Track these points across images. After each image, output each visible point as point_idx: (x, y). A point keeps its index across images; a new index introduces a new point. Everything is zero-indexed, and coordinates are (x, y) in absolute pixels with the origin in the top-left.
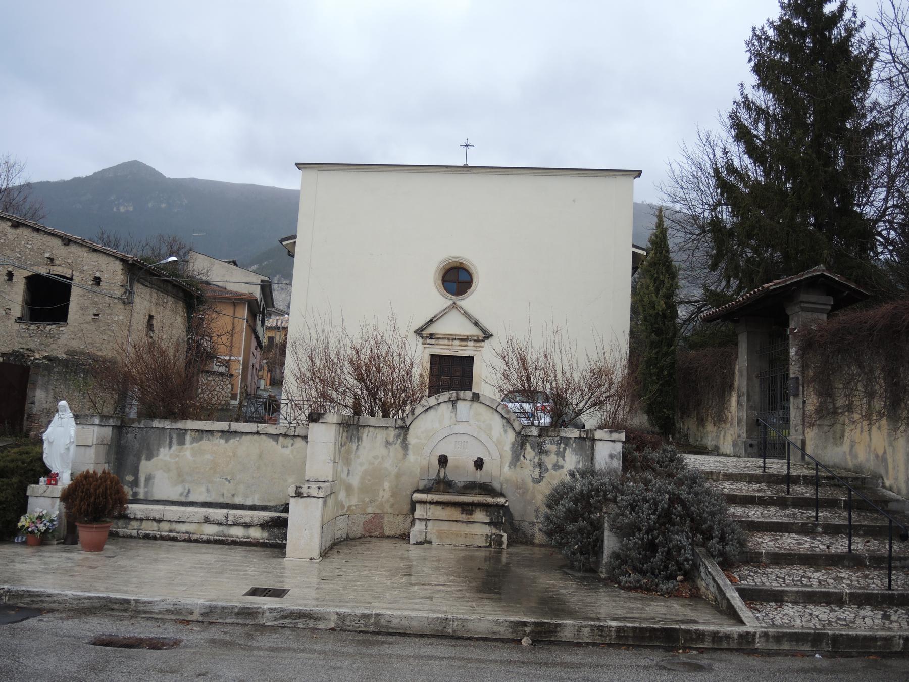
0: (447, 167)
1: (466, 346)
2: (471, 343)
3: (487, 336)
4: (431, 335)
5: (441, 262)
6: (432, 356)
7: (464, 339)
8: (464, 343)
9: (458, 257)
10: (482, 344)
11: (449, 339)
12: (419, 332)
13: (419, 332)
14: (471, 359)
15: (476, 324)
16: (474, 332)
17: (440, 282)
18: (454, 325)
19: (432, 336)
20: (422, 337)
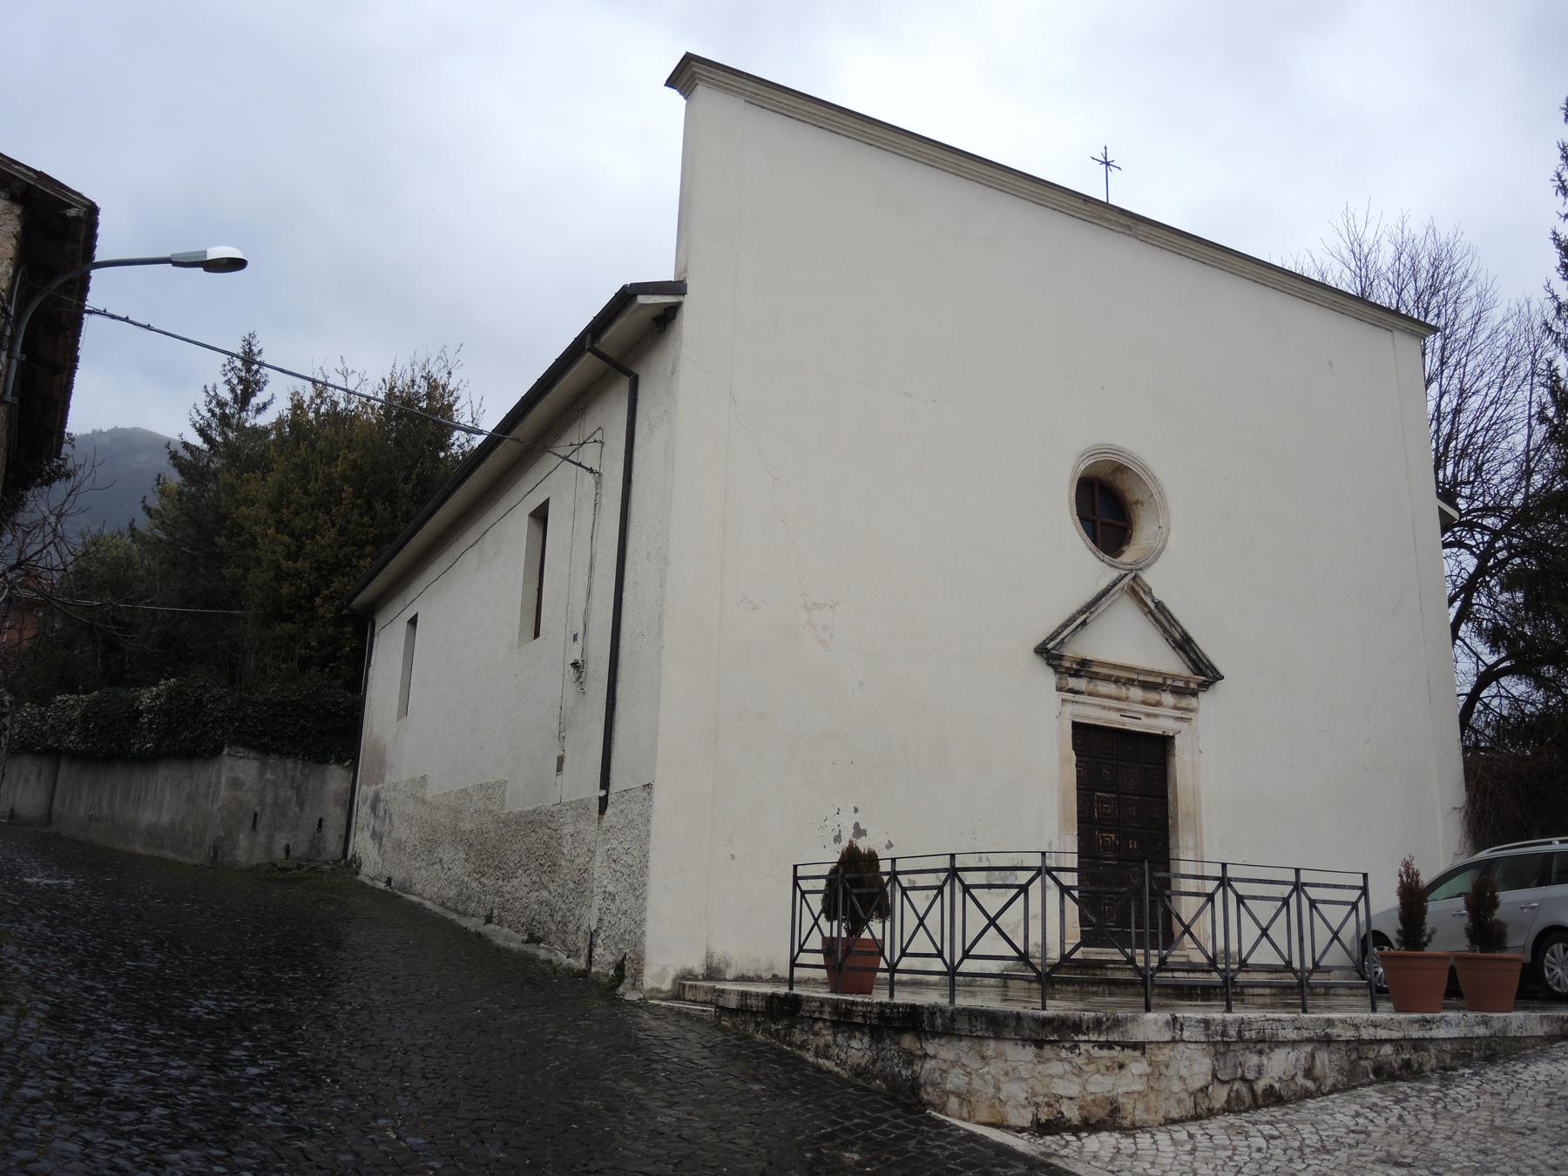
0: (1087, 199)
1: (1158, 704)
4: (1084, 663)
6: (1078, 728)
7: (1153, 684)
8: (1153, 696)
9: (1118, 452)
10: (1192, 702)
11: (1117, 681)
12: (1042, 651)
13: (1048, 653)
15: (1184, 644)
16: (1171, 663)
19: (1083, 668)
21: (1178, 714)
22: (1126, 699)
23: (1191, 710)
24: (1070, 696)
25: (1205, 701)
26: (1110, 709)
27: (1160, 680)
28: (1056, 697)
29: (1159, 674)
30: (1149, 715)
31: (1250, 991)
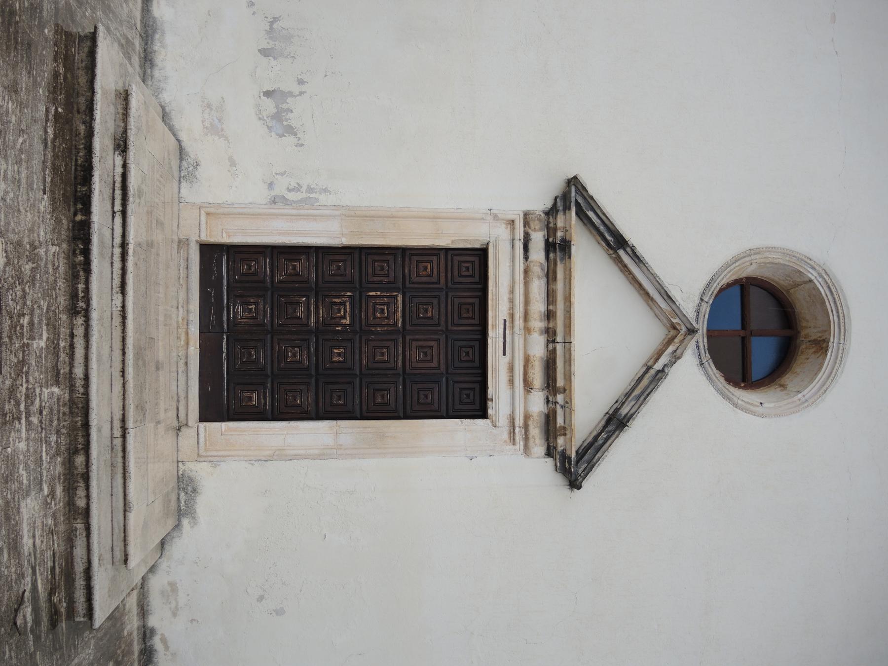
1: (528, 385)
2: (537, 404)
3: (574, 468)
4: (565, 247)
5: (825, 274)
6: (481, 254)
7: (553, 377)
8: (537, 377)
9: (844, 332)
10: (539, 448)
11: (550, 315)
12: (574, 198)
13: (574, 198)
14: (477, 406)
15: (616, 422)
16: (585, 415)
17: (750, 270)
18: (607, 332)
19: (558, 248)
20: (552, 212)
21: (519, 422)
22: (527, 330)
23: (526, 447)
24: (520, 233)
25: (541, 470)
26: (511, 301)
27: (560, 383)
28: (515, 211)
29: (568, 377)
30: (511, 369)
31: (79, 331)
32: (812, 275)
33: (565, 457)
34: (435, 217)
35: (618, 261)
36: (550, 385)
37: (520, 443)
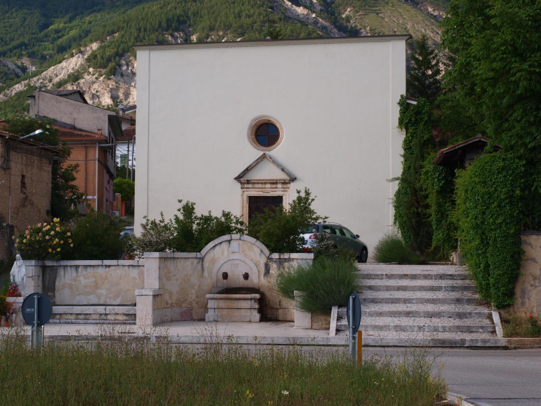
1: (276, 188)
4: (248, 181)
7: (274, 183)
8: (275, 186)
10: (289, 186)
11: (262, 183)
12: (238, 178)
17: (253, 137)
19: (248, 182)
20: (241, 183)
21: (283, 190)
22: (265, 188)
23: (289, 188)
24: (245, 190)
28: (240, 191)
30: (273, 191)
32: (253, 124)
33: (290, 180)
34: (243, 207)
35: (251, 169)
36: (276, 183)
37: (288, 189)
